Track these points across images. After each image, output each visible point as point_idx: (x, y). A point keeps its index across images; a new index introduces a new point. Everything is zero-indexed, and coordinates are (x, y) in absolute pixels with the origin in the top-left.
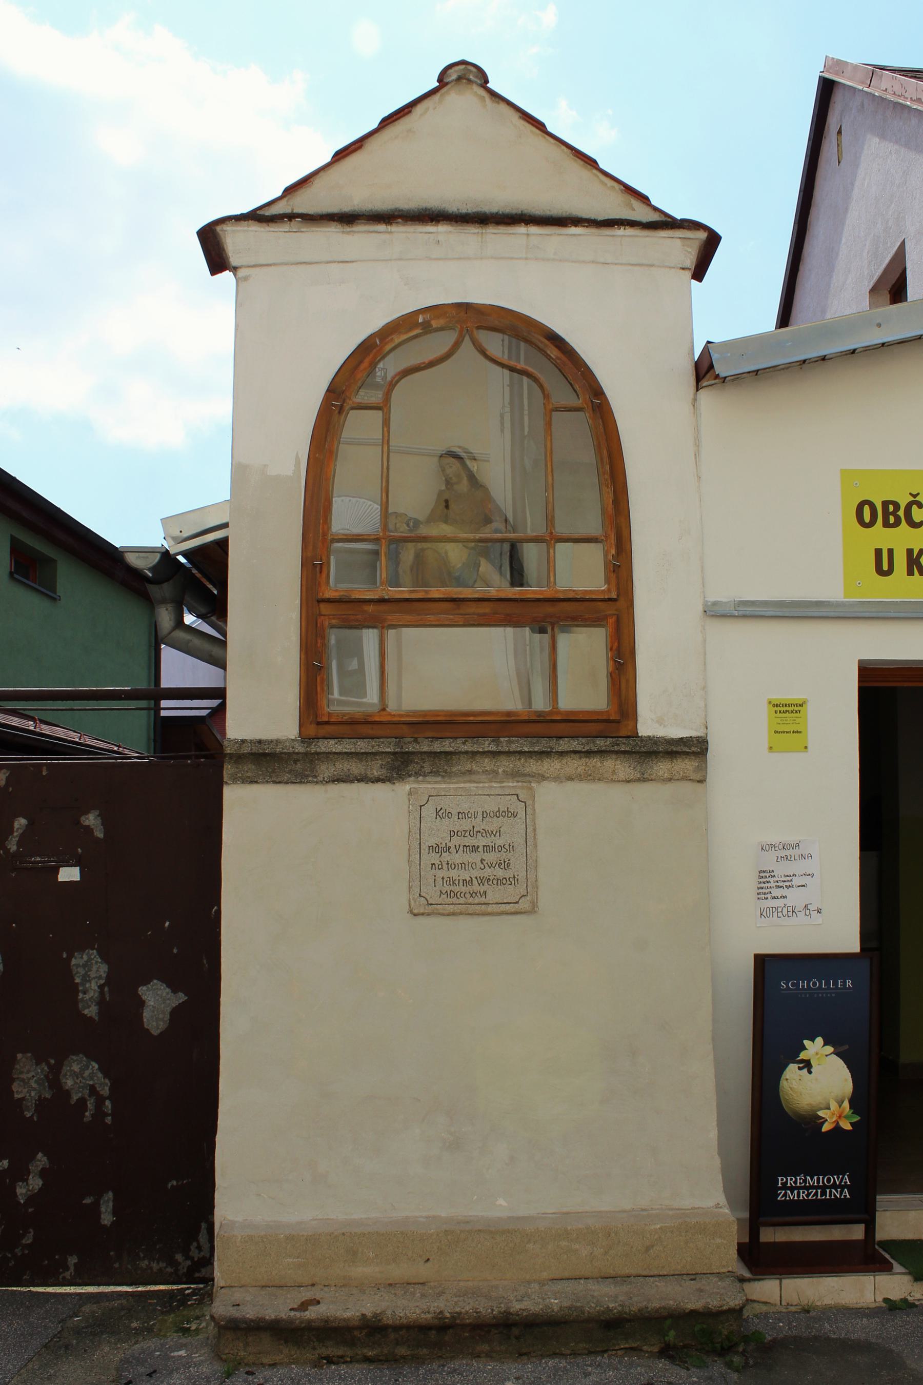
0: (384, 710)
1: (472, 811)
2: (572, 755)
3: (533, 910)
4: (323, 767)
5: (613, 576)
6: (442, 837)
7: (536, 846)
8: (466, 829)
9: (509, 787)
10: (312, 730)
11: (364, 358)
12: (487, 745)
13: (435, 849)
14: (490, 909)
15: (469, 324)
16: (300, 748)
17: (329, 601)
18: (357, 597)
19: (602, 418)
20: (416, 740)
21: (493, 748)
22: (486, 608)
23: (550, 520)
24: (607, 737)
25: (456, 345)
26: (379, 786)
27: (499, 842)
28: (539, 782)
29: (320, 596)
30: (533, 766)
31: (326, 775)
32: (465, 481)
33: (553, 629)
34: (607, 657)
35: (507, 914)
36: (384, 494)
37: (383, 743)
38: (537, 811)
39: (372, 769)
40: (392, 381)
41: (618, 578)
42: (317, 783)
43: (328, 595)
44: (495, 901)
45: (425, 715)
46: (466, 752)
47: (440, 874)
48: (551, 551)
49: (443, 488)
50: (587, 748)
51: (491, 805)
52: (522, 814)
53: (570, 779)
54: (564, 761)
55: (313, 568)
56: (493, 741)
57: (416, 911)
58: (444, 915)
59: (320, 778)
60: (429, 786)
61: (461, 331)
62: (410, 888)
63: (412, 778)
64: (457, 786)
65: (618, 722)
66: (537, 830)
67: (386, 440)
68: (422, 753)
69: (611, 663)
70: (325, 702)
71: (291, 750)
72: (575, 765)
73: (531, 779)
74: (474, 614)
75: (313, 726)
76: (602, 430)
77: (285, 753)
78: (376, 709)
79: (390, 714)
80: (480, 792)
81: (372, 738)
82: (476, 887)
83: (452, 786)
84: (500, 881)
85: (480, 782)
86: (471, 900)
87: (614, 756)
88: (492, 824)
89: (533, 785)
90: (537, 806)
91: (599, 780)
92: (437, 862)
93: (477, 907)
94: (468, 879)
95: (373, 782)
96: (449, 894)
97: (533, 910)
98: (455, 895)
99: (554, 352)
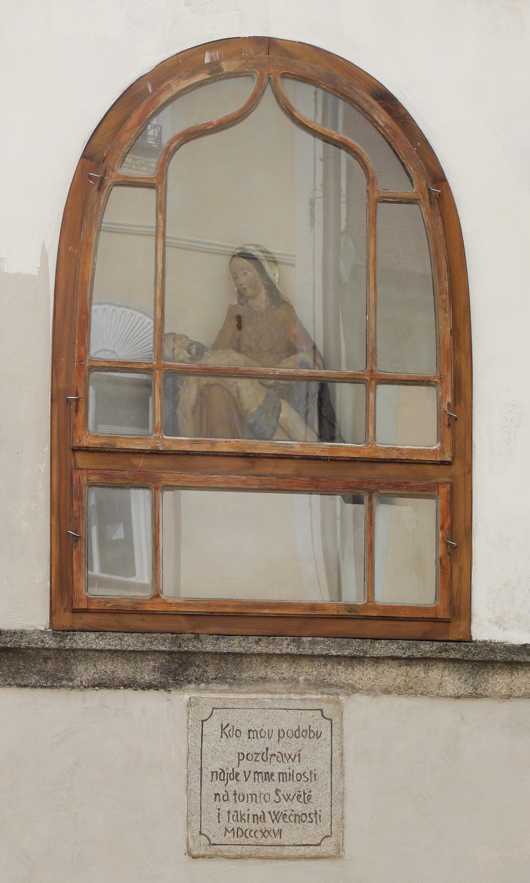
0: (157, 596)
1: (266, 729)
2: (390, 662)
3: (337, 855)
4: (81, 668)
5: (448, 432)
6: (229, 762)
7: (342, 774)
8: (258, 751)
9: (311, 700)
10: (66, 619)
11: (131, 112)
12: (286, 646)
13: (220, 775)
14: (286, 852)
15: (271, 71)
16: (51, 643)
17: (87, 450)
18: (124, 446)
19: (441, 215)
20: (197, 637)
21: (293, 649)
22: (287, 468)
23: (371, 354)
24: (433, 641)
25: (254, 100)
26: (152, 694)
27: (299, 769)
28: (349, 695)
29: (76, 443)
30: (342, 674)
31: (84, 678)
32: (263, 295)
33: (370, 499)
34: (437, 538)
35: (306, 858)
36: (158, 308)
37: (156, 639)
38: (346, 731)
39: (142, 673)
40: (168, 148)
41: (453, 434)
42: (73, 688)
43: (87, 441)
44: (292, 842)
45: (210, 605)
46: (260, 655)
47: (225, 807)
48: (371, 395)
49: (235, 302)
50: (408, 654)
51: (289, 721)
52: (326, 734)
53: (387, 691)
54: (380, 670)
55: (66, 405)
56: (293, 641)
57: (195, 853)
58: (229, 858)
59: (77, 682)
60: (214, 696)
61: (261, 80)
62: (188, 823)
63: (192, 686)
64: (248, 696)
65: (447, 621)
66: (345, 755)
67: (160, 233)
68: (205, 653)
69: (441, 545)
70: (83, 584)
71: (40, 645)
72: (392, 674)
73: (338, 691)
74: (272, 475)
75: (68, 614)
76: (441, 233)
77: (33, 649)
78: (147, 594)
79: (165, 602)
80: (276, 706)
81: (143, 633)
82: (269, 824)
83: (242, 696)
84: (299, 818)
85: (276, 693)
86: (262, 841)
87: (441, 665)
88: (291, 746)
89: (341, 698)
90: (345, 724)
91: (422, 694)
92: (222, 792)
93: (271, 850)
94: (260, 814)
95: (143, 689)
96: (236, 832)
97: (337, 855)
98: (244, 833)
99: (382, 117)
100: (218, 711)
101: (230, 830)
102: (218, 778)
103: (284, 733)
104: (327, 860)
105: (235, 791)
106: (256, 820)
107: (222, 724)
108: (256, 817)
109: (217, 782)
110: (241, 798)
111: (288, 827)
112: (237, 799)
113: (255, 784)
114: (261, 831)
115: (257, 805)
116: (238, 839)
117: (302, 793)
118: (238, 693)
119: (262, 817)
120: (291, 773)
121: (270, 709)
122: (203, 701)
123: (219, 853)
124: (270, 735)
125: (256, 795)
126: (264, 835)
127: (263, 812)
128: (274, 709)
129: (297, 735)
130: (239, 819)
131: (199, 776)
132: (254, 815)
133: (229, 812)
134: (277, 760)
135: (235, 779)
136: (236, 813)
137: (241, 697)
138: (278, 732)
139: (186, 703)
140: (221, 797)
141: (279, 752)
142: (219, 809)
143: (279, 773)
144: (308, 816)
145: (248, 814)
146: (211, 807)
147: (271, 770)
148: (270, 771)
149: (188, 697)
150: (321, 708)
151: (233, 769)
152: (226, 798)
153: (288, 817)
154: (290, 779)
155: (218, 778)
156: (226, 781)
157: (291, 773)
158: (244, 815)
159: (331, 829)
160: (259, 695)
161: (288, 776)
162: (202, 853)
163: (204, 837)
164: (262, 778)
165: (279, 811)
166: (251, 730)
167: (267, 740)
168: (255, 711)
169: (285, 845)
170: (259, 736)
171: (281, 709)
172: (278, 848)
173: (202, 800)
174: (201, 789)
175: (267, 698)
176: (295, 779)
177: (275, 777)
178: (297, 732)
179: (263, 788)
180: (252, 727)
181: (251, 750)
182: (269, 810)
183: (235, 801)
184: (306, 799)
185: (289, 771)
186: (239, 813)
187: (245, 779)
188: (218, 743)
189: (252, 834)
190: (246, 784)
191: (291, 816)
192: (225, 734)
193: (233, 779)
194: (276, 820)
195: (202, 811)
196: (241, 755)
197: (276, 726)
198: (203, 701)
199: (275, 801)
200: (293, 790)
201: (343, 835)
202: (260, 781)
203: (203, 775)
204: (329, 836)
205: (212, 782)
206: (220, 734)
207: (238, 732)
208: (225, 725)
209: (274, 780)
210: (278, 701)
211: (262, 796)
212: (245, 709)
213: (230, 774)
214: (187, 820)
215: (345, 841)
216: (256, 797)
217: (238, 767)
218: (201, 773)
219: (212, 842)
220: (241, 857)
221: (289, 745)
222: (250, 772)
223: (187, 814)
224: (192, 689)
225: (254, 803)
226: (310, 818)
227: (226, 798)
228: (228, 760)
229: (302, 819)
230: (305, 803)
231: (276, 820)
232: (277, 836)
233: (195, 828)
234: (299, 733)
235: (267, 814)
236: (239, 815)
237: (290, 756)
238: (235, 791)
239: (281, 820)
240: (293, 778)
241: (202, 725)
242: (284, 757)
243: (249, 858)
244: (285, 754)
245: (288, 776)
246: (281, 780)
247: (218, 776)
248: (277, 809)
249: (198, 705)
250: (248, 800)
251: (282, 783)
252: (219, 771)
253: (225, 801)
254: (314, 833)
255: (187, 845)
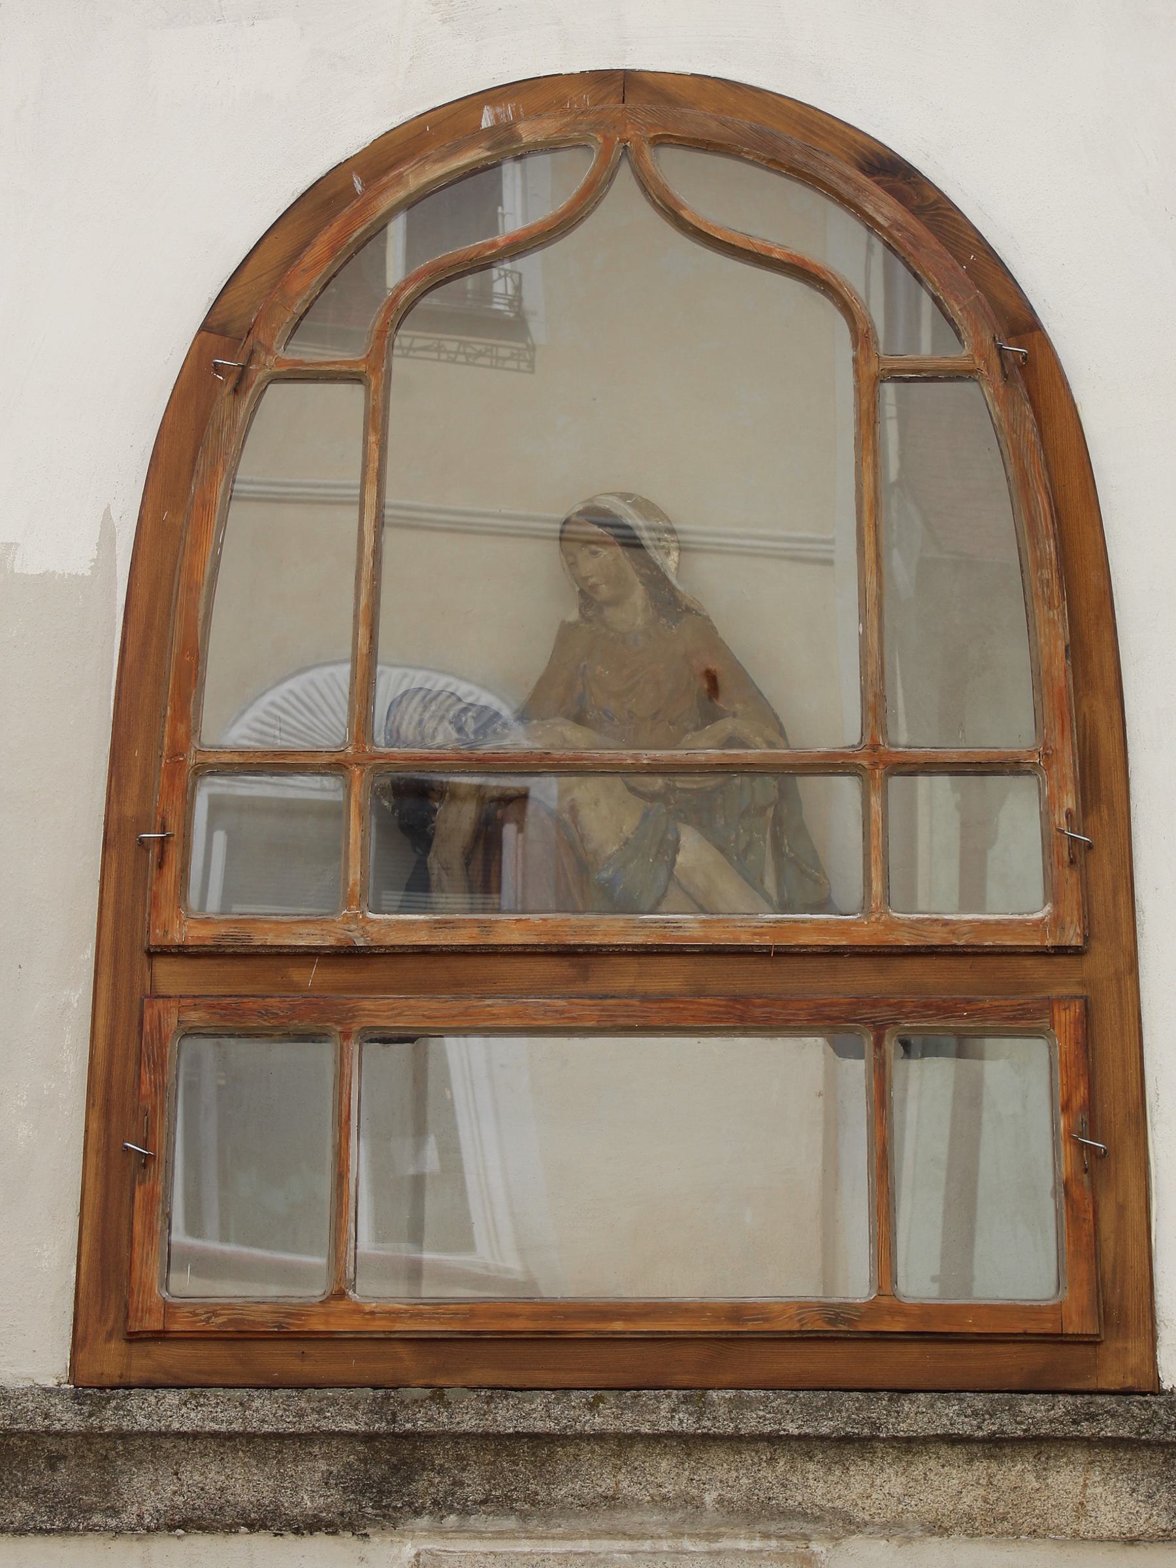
0: (340, 1295)
2: (944, 1450)
4: (141, 1480)
5: (1071, 878)
10: (111, 1359)
11: (315, 233)
12: (666, 1413)
15: (630, 133)
16: (68, 1419)
17: (182, 952)
18: (271, 940)
19: (1031, 400)
20: (438, 1394)
21: (684, 1422)
22: (669, 978)
24: (1054, 1392)
25: (590, 196)
26: (319, 1546)
28: (835, 1539)
29: (157, 937)
30: (815, 1484)
31: (148, 1506)
33: (879, 1043)
34: (1055, 1133)
36: (363, 632)
37: (333, 1402)
39: (296, 1489)
40: (395, 299)
41: (1085, 886)
42: (118, 1532)
43: (181, 933)
45: (472, 1314)
46: (600, 1437)
48: (875, 801)
50: (989, 1427)
53: (937, 1528)
54: (918, 1471)
56: (686, 1400)
59: (128, 1517)
60: (479, 1546)
61: (605, 153)
63: (424, 1521)
64: (568, 1546)
65: (1092, 1342)
67: (375, 472)
68: (458, 1437)
69: (1067, 1150)
70: (155, 1270)
71: (40, 1423)
72: (951, 1483)
73: (808, 1528)
74: (632, 995)
75: (116, 1346)
76: (1033, 437)
77: (22, 1435)
78: (317, 1291)
79: (358, 1310)
81: (301, 1387)
83: (552, 1547)
85: (643, 1537)
87: (1080, 1456)
89: (815, 1547)
91: (1033, 1533)
95: (297, 1532)
99: (885, 209)
118: (542, 1538)
137: (552, 1550)
149: (413, 1552)
160: (597, 1542)
175: (619, 1552)
210: (650, 1557)
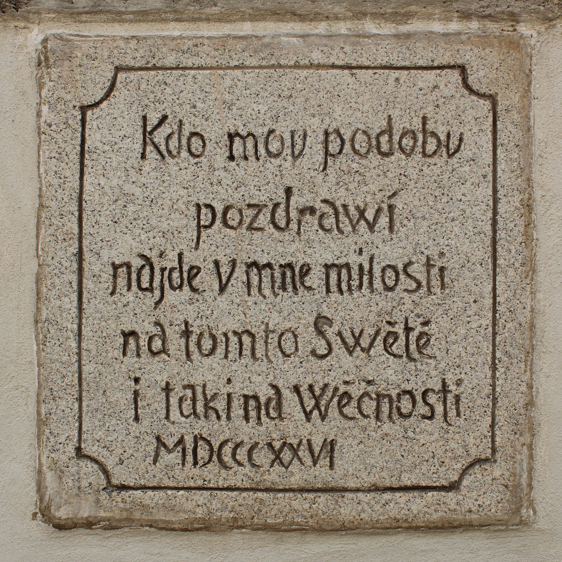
1: (283, 128)
3: (514, 516)
6: (166, 231)
8: (261, 198)
9: (429, 36)
13: (141, 275)
14: (348, 509)
35: (412, 527)
44: (368, 480)
47: (156, 372)
51: (359, 105)
57: (62, 514)
58: (167, 528)
62: (42, 422)
64: (226, 29)
80: (317, 57)
82: (295, 425)
84: (391, 405)
85: (316, 17)
86: (274, 476)
88: (367, 182)
89: (524, 29)
92: (145, 327)
93: (300, 503)
94: (265, 393)
96: (191, 450)
97: (514, 516)
98: (216, 453)
100: (133, 76)
101: (170, 442)
102: (134, 284)
103: (343, 142)
104: (478, 533)
105: (186, 323)
106: (253, 414)
107: (145, 118)
108: (252, 403)
109: (130, 297)
110: (207, 344)
111: (356, 432)
112: (193, 347)
113: (251, 300)
114: (270, 445)
115: (256, 367)
116: (196, 471)
117: (399, 329)
119: (273, 403)
120: (366, 267)
121: (297, 66)
122: (85, 46)
123: (137, 515)
124: (298, 148)
125: (252, 335)
126: (278, 457)
127: (274, 387)
128: (311, 66)
129: (385, 147)
130: (200, 408)
131: (74, 278)
132: (246, 397)
133: (167, 389)
134: (322, 227)
135: (186, 288)
136: (189, 393)
137: (206, 33)
138: (321, 138)
139: (34, 55)
140: (143, 342)
141: (325, 201)
142: (137, 380)
143: (327, 266)
144: (419, 398)
145: (229, 395)
146: (111, 373)
147: (300, 256)
148: (299, 260)
149: (41, 38)
150: (460, 62)
151: (180, 256)
152: (157, 344)
153: (354, 403)
154: (360, 286)
155: (134, 284)
156: (157, 293)
157: (366, 267)
158: (215, 396)
159: (493, 437)
160: (261, 25)
161: (355, 276)
162: (85, 512)
163: (89, 464)
164: (273, 282)
165: (326, 386)
166: (238, 134)
167: (288, 164)
168: (250, 76)
169: (345, 490)
170: (262, 150)
171: (333, 66)
172: (323, 498)
173: (84, 353)
174: (80, 318)
175: (288, 35)
176: (378, 284)
177: (315, 279)
178: (384, 139)
179: (275, 315)
180: (239, 123)
181: (237, 195)
182: (294, 381)
183: (188, 355)
184: (413, 347)
185: (359, 260)
186: (199, 390)
187: (216, 287)
188: (134, 175)
189: (242, 454)
190: (223, 301)
191: (366, 399)
192: (156, 147)
193: (180, 287)
194: (316, 413)
195: (85, 386)
196: (204, 210)
197: (316, 121)
198: (85, 46)
199: (313, 353)
200: (373, 318)
201: (531, 457)
202: (267, 292)
203: (87, 273)
204: (487, 460)
205: (116, 297)
206: (138, 147)
207: (196, 143)
208: (153, 120)
209: (309, 288)
210: (324, 41)
211: (273, 339)
212: (219, 68)
213: (172, 270)
214: (39, 413)
215: (536, 475)
216: (253, 342)
217: (197, 247)
218: (80, 270)
219: (115, 481)
220: (206, 526)
221: (358, 178)
222: (233, 263)
223: (38, 395)
224: (50, 11)
225: (247, 359)
226: (427, 404)
227: (157, 344)
228: (164, 226)
229: (399, 409)
230: (411, 359)
231: (316, 413)
232: (321, 462)
233: (62, 439)
234: (390, 141)
235: (287, 394)
236: (200, 396)
237: (362, 213)
238: (186, 323)
239: (333, 412)
240: (371, 283)
241: (83, 121)
242: (342, 217)
243: (232, 528)
244: (345, 206)
245: (355, 276)
246: (334, 288)
247: (134, 276)
248: (319, 377)
249: (70, 58)
250: (227, 352)
251: (335, 296)
252: (137, 263)
253: (154, 354)
254: (440, 452)
255: (38, 491)
